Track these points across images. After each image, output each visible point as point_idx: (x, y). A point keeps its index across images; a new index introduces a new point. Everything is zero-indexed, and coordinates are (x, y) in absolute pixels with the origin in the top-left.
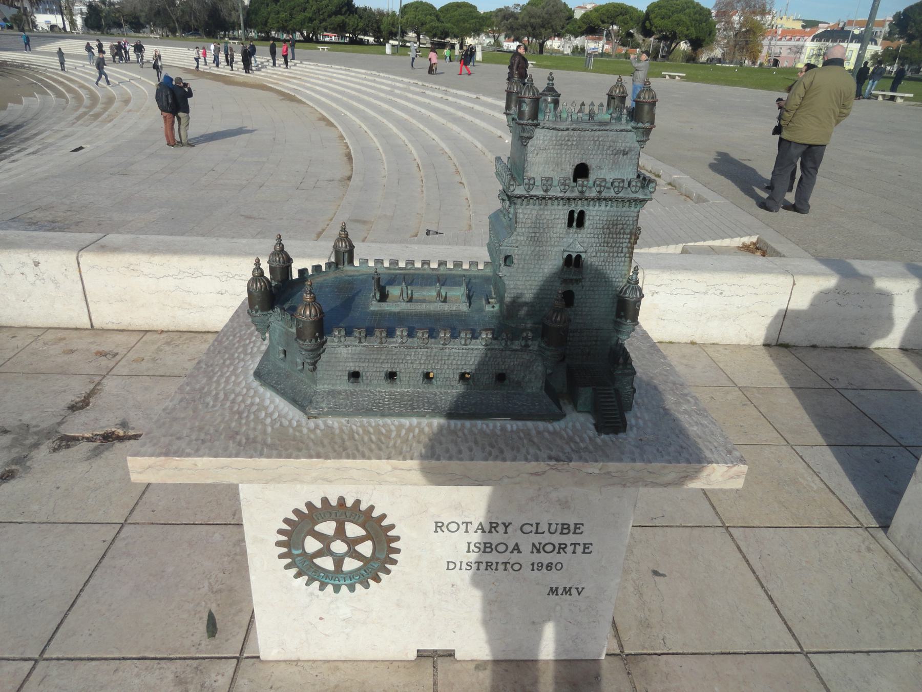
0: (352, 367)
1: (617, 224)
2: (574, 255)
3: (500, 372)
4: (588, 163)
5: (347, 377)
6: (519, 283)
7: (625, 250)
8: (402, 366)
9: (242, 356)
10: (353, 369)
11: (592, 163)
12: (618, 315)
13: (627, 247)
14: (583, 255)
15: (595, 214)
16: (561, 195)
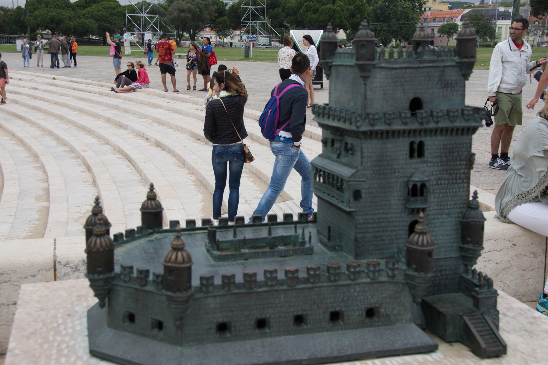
0: (220, 318)
1: (453, 152)
2: (419, 185)
3: (369, 306)
4: (420, 96)
5: (214, 331)
6: (368, 217)
7: (463, 176)
8: (270, 311)
9: (59, 338)
10: (220, 320)
11: (424, 96)
12: (463, 240)
13: (464, 173)
14: (427, 184)
15: (432, 144)
16: (403, 127)
